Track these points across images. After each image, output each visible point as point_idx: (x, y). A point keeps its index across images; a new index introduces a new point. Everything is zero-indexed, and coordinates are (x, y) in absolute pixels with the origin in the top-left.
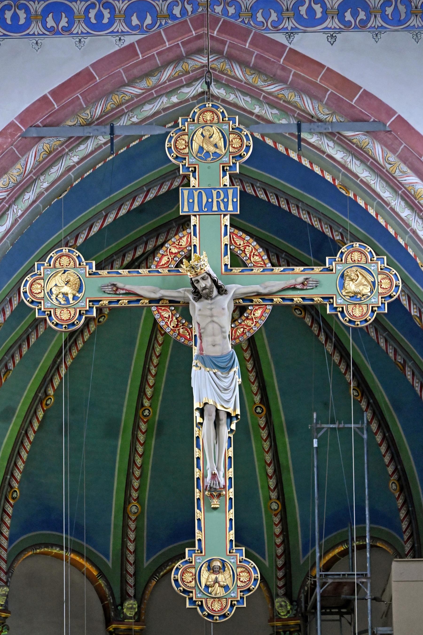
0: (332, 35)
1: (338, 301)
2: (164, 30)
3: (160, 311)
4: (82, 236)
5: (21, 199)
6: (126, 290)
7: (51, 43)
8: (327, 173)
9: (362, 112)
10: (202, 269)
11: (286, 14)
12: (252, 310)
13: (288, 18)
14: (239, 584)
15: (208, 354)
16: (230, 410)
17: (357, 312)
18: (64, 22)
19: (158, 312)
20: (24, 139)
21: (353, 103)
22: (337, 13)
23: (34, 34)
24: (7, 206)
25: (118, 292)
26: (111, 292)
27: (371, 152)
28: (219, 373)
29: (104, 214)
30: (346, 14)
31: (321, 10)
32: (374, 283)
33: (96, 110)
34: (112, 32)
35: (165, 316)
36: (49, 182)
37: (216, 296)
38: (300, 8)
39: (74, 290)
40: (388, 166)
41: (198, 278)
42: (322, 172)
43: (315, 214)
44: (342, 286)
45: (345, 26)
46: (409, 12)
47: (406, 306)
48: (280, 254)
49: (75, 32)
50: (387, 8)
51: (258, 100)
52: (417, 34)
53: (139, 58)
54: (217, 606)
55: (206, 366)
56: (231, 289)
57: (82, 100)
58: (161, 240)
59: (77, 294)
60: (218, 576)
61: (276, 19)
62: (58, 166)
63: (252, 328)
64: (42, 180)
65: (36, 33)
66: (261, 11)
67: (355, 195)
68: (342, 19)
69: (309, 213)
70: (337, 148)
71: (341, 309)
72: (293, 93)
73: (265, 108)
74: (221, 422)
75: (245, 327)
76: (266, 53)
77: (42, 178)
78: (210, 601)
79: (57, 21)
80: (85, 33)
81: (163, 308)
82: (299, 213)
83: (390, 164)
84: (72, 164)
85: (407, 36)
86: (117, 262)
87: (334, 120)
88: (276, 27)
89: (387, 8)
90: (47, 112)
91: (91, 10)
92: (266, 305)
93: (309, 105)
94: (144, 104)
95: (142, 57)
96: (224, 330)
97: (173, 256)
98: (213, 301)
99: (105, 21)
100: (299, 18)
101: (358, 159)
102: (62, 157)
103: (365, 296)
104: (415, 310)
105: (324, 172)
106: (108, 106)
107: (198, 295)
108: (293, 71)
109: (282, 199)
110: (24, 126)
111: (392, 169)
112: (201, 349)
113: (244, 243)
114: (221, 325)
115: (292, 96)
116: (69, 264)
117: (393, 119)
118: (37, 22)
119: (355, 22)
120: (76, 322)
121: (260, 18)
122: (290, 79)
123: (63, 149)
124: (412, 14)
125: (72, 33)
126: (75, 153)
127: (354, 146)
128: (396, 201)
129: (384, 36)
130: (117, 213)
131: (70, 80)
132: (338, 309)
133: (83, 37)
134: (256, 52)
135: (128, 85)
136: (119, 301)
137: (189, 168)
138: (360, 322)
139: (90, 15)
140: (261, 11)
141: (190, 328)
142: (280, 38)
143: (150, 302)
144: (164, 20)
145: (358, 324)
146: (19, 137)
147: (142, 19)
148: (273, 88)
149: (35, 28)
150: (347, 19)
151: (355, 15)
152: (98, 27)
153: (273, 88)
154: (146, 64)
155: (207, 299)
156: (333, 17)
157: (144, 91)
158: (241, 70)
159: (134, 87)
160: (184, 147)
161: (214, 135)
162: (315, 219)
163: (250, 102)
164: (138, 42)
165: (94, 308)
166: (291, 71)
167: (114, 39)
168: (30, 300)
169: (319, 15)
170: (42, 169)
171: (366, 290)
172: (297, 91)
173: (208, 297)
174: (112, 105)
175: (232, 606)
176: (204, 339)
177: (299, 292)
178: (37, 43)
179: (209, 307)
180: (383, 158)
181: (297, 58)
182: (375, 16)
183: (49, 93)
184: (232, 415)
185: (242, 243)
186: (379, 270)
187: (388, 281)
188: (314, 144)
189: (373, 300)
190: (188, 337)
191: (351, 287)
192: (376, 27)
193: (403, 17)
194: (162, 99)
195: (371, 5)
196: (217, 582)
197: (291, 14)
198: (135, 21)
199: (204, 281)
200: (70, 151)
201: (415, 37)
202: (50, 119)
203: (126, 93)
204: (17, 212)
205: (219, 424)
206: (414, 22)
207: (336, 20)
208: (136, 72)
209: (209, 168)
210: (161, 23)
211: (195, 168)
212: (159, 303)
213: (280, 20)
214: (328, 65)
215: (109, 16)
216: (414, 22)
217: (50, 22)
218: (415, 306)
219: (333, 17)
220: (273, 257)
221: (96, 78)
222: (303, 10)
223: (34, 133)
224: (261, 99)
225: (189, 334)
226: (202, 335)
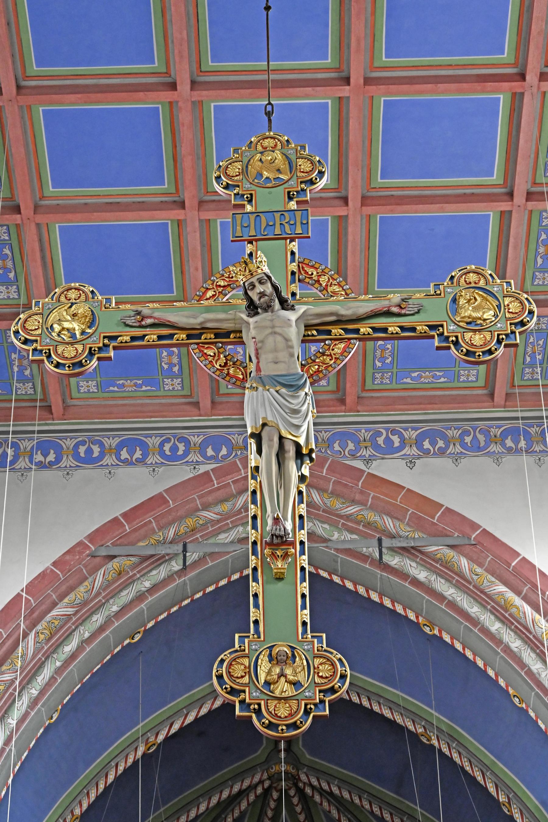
0: (411, 461)
1: (450, 329)
2: (239, 460)
3: (202, 349)
4: (163, 732)
5: (88, 621)
6: (155, 318)
7: (123, 472)
8: (410, 611)
9: (446, 529)
10: (258, 267)
11: (363, 444)
12: (329, 345)
13: (366, 447)
14: (317, 680)
15: (267, 374)
16: (302, 441)
17: (478, 339)
18: (138, 454)
19: (201, 351)
20: (93, 558)
21: (435, 521)
22: (415, 442)
23: (107, 465)
24: (73, 627)
25: (143, 323)
26: (135, 324)
27: (456, 565)
28: (283, 391)
29: (186, 713)
30: (424, 443)
31: (399, 440)
32: (499, 307)
33: (169, 531)
34: (187, 462)
35: (208, 353)
36: (120, 605)
37: (278, 310)
38: (378, 439)
39: (83, 324)
40: (475, 577)
41: (254, 280)
42: (405, 610)
43: (396, 709)
44: (456, 312)
45: (424, 453)
46: (488, 440)
47: (493, 794)
48: (362, 795)
49: (149, 463)
50: (465, 437)
51: (337, 527)
52: (497, 458)
53: (214, 485)
54: (283, 711)
55: (264, 386)
56: (300, 309)
57: (154, 525)
58: (246, 784)
59: (88, 331)
60: (284, 667)
61: (354, 448)
62: (128, 590)
63: (331, 365)
64: (111, 603)
65: (110, 464)
66: (338, 442)
67: (440, 631)
68: (420, 446)
69: (390, 709)
70: (420, 568)
71: (454, 339)
72: (373, 513)
73: (344, 534)
74: (286, 455)
75: (321, 364)
76: (343, 478)
77: (111, 601)
78: (272, 704)
79: (131, 453)
80: (160, 464)
81: (206, 346)
82: (381, 709)
83: (477, 575)
84: (144, 589)
85: (488, 461)
86: (203, 805)
87: (417, 536)
88: (353, 456)
89: (465, 437)
90: (117, 533)
91: (165, 444)
92: (349, 339)
93: (389, 524)
94: (219, 533)
95: (218, 484)
96: (290, 343)
97: (220, 289)
98: (274, 313)
99: (180, 452)
100: (376, 447)
101: (442, 577)
102: (134, 581)
103: (488, 321)
104: (503, 796)
105: (407, 609)
106: (182, 528)
107: (253, 308)
108: (372, 494)
109: (363, 696)
110: (93, 544)
111: (479, 580)
112: (258, 369)
113: (317, 273)
114: (286, 336)
115: (372, 516)
116: (79, 297)
117: (478, 532)
118: (111, 455)
119: (434, 450)
120: (84, 361)
121: (337, 447)
122: (369, 503)
123: (135, 575)
124: (491, 442)
125: (146, 464)
126: (146, 577)
127: (438, 566)
128: (486, 615)
129: (464, 462)
130: (199, 712)
131: (143, 503)
132: (451, 339)
133: (157, 467)
134: (334, 479)
135: (202, 510)
136: (145, 336)
137: (244, 195)
138: (483, 352)
139: (164, 448)
140: (338, 442)
141: (243, 368)
142: (359, 464)
143: (189, 337)
144: (240, 451)
145: (479, 355)
146: (88, 556)
147: (217, 450)
148: (352, 510)
149: (108, 460)
150: (425, 447)
151: (433, 443)
152: (173, 457)
153: (352, 510)
154: (221, 491)
155: (265, 310)
156: (411, 446)
157: (219, 517)
158: (319, 495)
159: (208, 511)
160: (238, 174)
161: (277, 161)
162: (397, 713)
163: (329, 529)
164: (212, 470)
165: (111, 347)
166: (370, 494)
167: (188, 468)
168: (23, 338)
169: (397, 444)
170: (111, 591)
171: (489, 315)
172: (377, 511)
173: (268, 308)
174: (186, 528)
175: (307, 712)
176: (263, 358)
177: (395, 319)
178: (110, 473)
179: (270, 318)
180: (469, 570)
181: (376, 481)
182: (454, 444)
183: (120, 515)
184: (305, 451)
185: (315, 273)
186: (505, 292)
187: (517, 304)
188: (396, 566)
189: (499, 325)
190: (241, 377)
191: (468, 312)
192: (456, 453)
193: (482, 444)
194: (238, 528)
195: (449, 435)
196: (282, 675)
197: (369, 444)
198: (210, 452)
199: (262, 286)
200: (141, 576)
201: (496, 461)
202: (121, 540)
203: (201, 517)
204: (84, 633)
205: (284, 459)
206: (494, 449)
207: (415, 448)
208: (210, 499)
209: (270, 193)
210: (236, 453)
211: (251, 195)
212: (200, 339)
213: (358, 449)
214: (407, 486)
215: (184, 448)
216: (494, 449)
217: (124, 454)
218: (503, 793)
219: (411, 446)
220: (356, 798)
221: (169, 502)
222: (380, 441)
223: (103, 552)
224: (340, 527)
225: (242, 374)
226: (260, 351)
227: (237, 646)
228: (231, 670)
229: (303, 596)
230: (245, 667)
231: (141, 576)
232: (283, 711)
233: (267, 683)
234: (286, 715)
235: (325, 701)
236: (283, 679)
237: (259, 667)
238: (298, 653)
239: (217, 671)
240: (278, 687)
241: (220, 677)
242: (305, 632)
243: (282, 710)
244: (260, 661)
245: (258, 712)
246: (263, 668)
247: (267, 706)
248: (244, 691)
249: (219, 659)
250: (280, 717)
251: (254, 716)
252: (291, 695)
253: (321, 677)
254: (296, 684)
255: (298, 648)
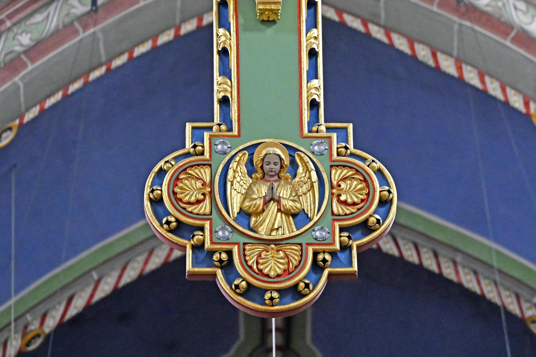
14: (337, 208)
54: (273, 265)
60: (276, 185)
78: (253, 252)
126: (23, 26)
175: (317, 267)
196: (272, 199)
200: (14, 25)
227: (189, 144)
228: (177, 190)
229: (313, 53)
230: (204, 184)
231: (14, 25)
232: (273, 265)
233: (245, 214)
234: (279, 272)
235: (350, 248)
236: (273, 207)
237: (229, 184)
238: (301, 159)
239: (152, 191)
240: (264, 221)
241: (157, 202)
242: (314, 120)
243: (272, 263)
244: (231, 173)
245: (228, 266)
246: (236, 186)
247: (243, 255)
248: (202, 229)
249: (156, 169)
250: (267, 276)
251: (219, 272)
252: (287, 235)
253: (345, 203)
254: (298, 216)
255: (302, 149)
